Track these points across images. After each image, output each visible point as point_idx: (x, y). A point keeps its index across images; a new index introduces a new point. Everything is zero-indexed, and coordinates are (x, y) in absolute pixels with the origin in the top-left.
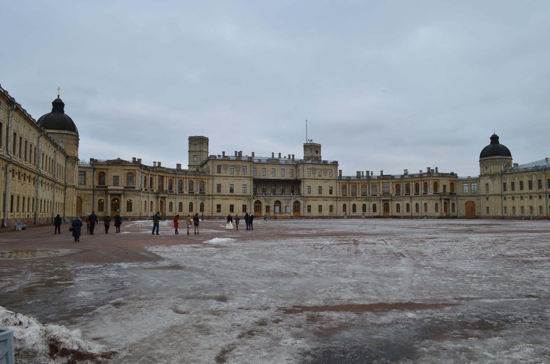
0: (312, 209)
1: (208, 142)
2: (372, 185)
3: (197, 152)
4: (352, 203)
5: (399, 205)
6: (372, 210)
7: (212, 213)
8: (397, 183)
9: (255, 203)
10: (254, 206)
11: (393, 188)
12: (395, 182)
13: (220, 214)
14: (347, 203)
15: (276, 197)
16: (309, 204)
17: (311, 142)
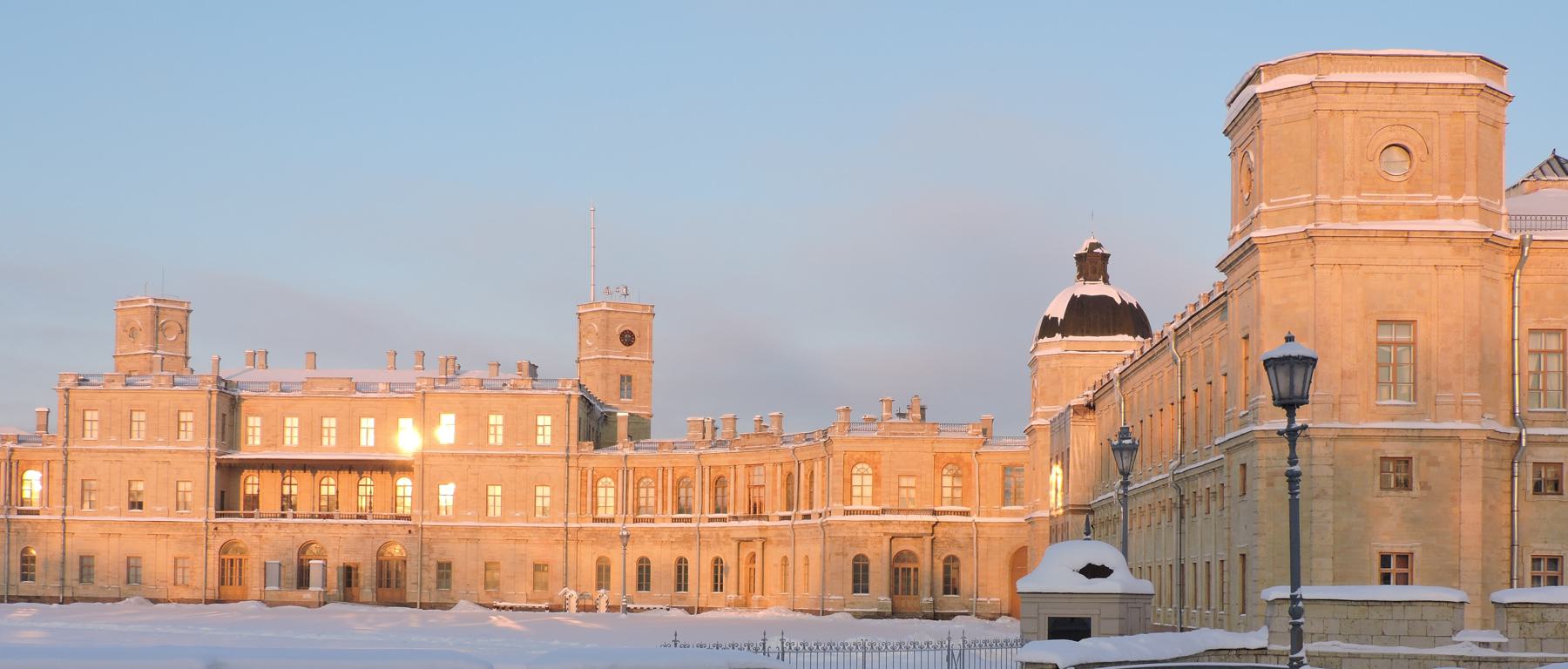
0: (455, 576)
1: (187, 318)
2: (714, 475)
3: (136, 358)
4: (635, 553)
5: (686, 562)
6: (707, 583)
7: (63, 587)
8: (787, 468)
9: (224, 549)
10: (222, 562)
11: (774, 491)
12: (781, 464)
13: (90, 591)
14: (615, 556)
15: (307, 530)
16: (444, 559)
17: (623, 300)
